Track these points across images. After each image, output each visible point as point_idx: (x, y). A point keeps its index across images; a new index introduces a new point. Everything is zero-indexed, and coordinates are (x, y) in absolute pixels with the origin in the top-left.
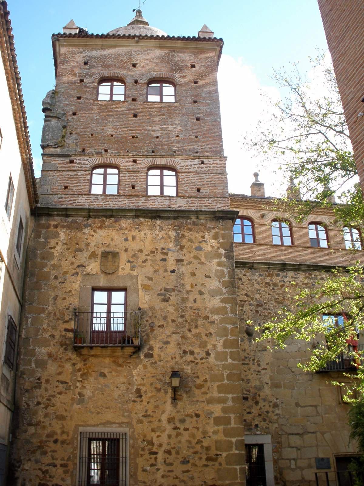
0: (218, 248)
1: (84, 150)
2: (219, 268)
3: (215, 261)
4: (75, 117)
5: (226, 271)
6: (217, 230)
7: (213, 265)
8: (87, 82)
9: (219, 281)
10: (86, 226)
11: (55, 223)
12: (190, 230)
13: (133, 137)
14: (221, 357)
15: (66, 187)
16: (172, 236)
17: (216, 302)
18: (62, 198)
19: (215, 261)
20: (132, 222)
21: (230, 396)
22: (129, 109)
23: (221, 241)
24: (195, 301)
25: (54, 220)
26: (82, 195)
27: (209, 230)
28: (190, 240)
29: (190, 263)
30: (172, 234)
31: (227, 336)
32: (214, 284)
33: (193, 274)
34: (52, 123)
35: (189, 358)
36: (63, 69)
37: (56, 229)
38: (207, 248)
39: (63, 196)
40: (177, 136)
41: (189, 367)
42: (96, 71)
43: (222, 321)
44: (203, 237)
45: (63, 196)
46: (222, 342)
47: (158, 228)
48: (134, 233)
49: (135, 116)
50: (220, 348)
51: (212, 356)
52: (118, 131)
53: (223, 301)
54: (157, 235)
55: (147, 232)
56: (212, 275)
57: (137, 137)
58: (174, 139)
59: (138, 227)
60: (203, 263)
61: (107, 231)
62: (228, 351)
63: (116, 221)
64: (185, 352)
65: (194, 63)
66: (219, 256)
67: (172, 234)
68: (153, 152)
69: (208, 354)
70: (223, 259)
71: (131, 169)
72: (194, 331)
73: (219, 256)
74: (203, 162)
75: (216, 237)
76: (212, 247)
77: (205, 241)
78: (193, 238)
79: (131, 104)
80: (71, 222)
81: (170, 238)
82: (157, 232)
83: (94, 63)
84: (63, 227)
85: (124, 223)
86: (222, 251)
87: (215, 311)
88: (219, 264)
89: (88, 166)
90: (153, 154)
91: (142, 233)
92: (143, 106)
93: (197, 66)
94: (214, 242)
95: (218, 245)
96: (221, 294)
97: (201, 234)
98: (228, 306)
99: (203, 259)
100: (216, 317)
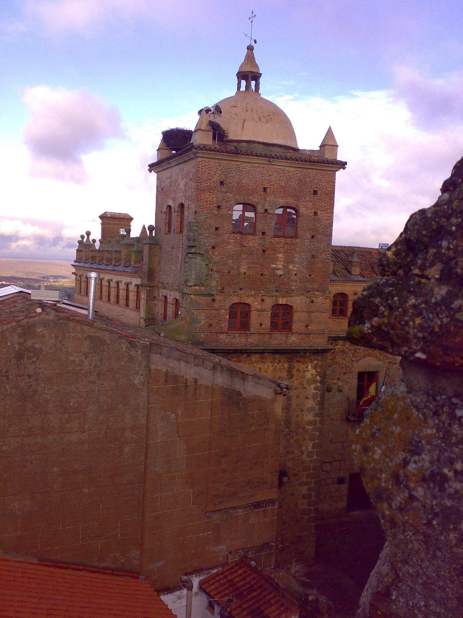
0: (316, 376)
2: (314, 391)
3: (313, 386)
5: (319, 393)
6: (316, 362)
7: (311, 390)
9: (314, 400)
12: (298, 361)
14: (310, 454)
16: (286, 368)
17: (310, 417)
19: (313, 386)
20: (259, 356)
21: (313, 480)
23: (319, 370)
24: (297, 416)
26: (223, 333)
27: (311, 362)
28: (298, 370)
29: (296, 388)
30: (286, 365)
31: (314, 440)
32: (310, 403)
33: (298, 397)
35: (290, 456)
36: (201, 190)
38: (308, 375)
40: (296, 275)
41: (290, 463)
42: (232, 195)
43: (314, 429)
44: (307, 367)
46: (312, 444)
47: (277, 361)
48: (260, 365)
50: (310, 449)
51: (305, 454)
53: (315, 415)
54: (276, 367)
55: (269, 364)
56: (310, 397)
58: (293, 277)
59: (262, 360)
60: (305, 388)
62: (315, 450)
63: (248, 356)
64: (288, 452)
65: (316, 189)
66: (315, 382)
67: (286, 365)
68: (277, 291)
69: (302, 453)
70: (319, 384)
72: (295, 438)
73: (315, 382)
74: (312, 301)
75: (315, 367)
76: (312, 375)
77: (308, 371)
78: (300, 368)
81: (285, 368)
82: (276, 364)
85: (255, 358)
86: (318, 378)
87: (310, 423)
88: (315, 388)
90: (277, 294)
91: (266, 365)
93: (319, 192)
94: (313, 371)
95: (316, 373)
96: (315, 410)
97: (306, 365)
98: (318, 419)
99: (305, 384)
100: (310, 427)
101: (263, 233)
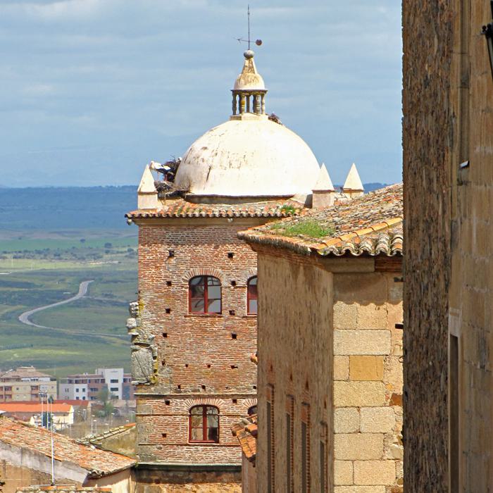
1: (179, 387)
4: (167, 341)
8: (175, 286)
10: (188, 481)
11: (156, 478)
13: (233, 367)
15: (164, 435)
18: (161, 448)
20: (233, 476)
22: (227, 328)
25: (156, 475)
34: (141, 352)
37: (157, 485)
39: (161, 446)
45: (161, 446)
49: (234, 336)
52: (215, 360)
57: (237, 367)
61: (208, 486)
63: (217, 476)
71: (231, 412)
79: (228, 319)
80: (173, 476)
83: (182, 254)
84: (165, 482)
89: (185, 409)
92: (242, 323)
101: (232, 313)
